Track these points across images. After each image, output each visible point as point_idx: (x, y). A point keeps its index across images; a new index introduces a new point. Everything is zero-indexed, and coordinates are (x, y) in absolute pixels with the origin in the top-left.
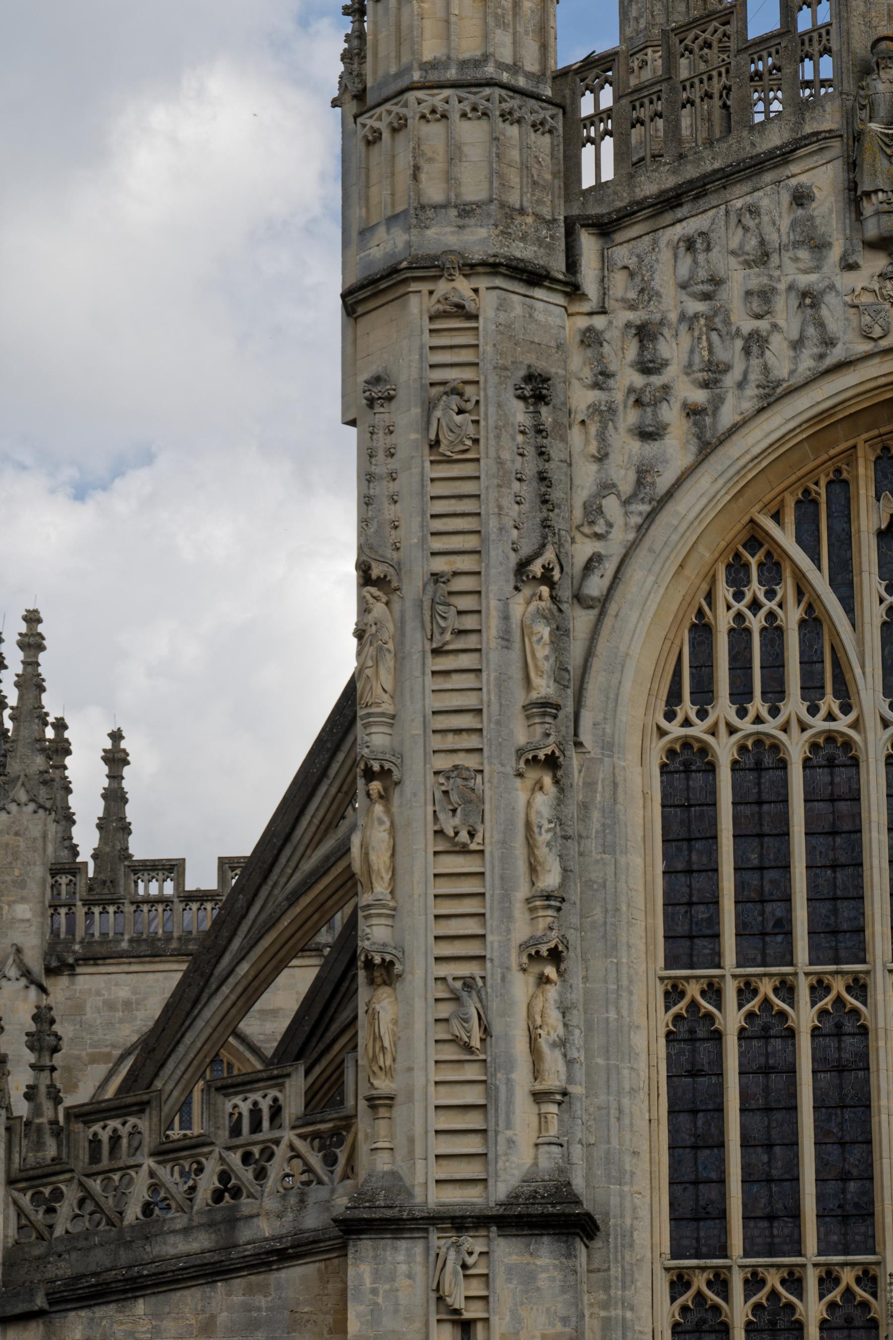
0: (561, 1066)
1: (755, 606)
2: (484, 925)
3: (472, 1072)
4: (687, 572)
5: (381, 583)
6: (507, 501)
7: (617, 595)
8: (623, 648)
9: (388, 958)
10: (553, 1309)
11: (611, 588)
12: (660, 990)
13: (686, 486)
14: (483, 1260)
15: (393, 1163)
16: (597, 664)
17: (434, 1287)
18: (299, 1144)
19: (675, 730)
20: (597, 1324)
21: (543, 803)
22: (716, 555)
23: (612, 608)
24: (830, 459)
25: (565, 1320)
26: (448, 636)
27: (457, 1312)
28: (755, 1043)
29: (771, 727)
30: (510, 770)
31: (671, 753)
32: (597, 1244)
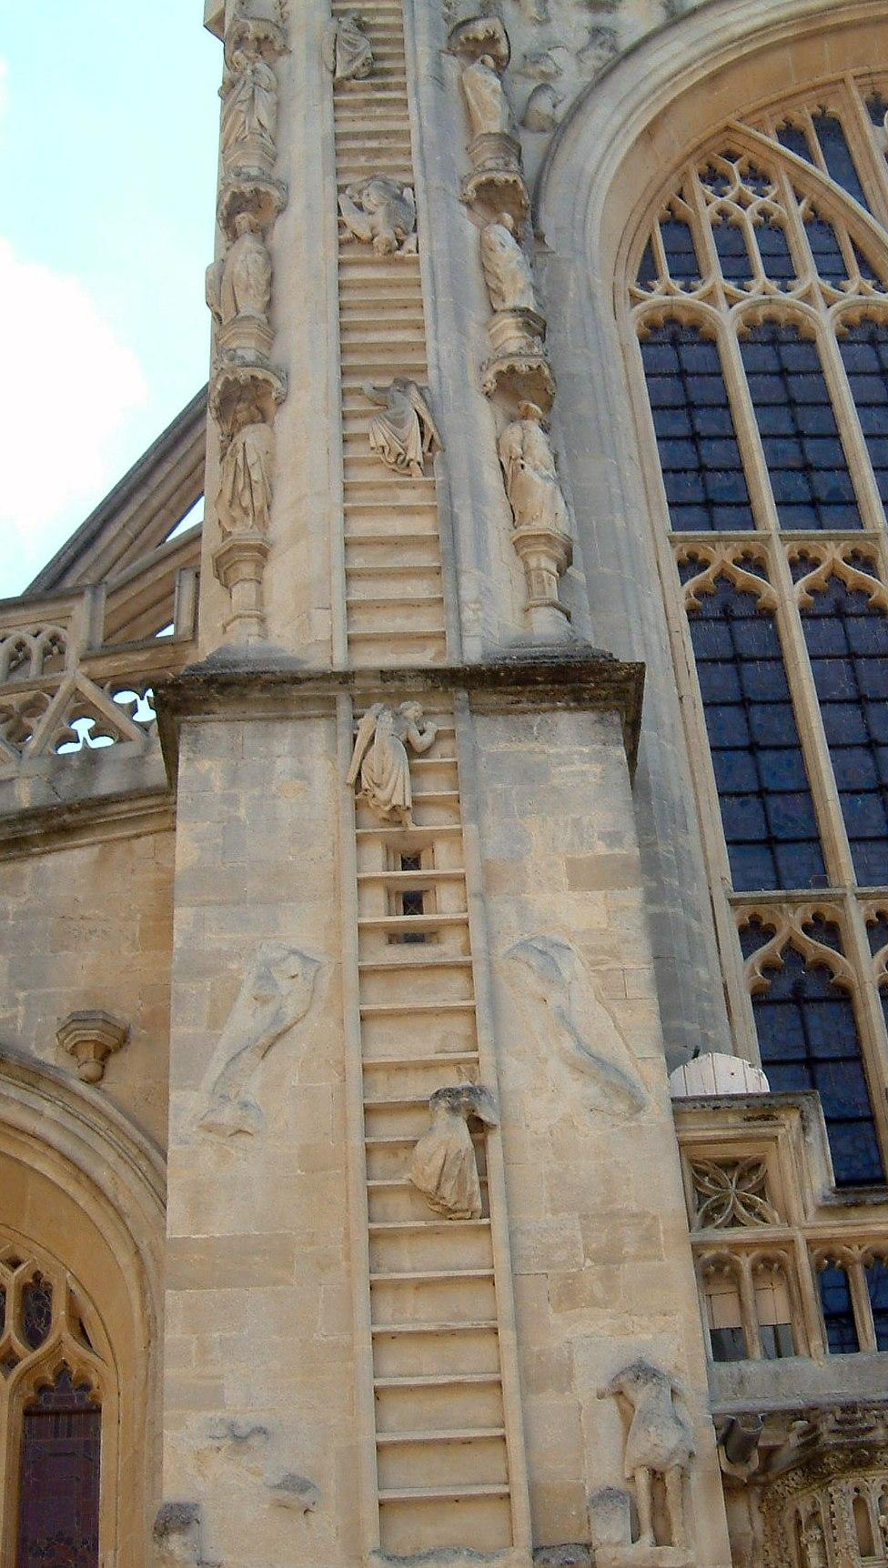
1: (742, 202)
2: (423, 335)
8: (590, 167)
9: (260, 374)
10: (585, 820)
13: (655, 44)
14: (445, 746)
15: (264, 635)
17: (352, 778)
19: (656, 298)
21: (501, 234)
22: (688, 148)
23: (571, 133)
24: (814, 88)
25: (613, 838)
26: (358, 63)
28: (824, 622)
31: (652, 326)
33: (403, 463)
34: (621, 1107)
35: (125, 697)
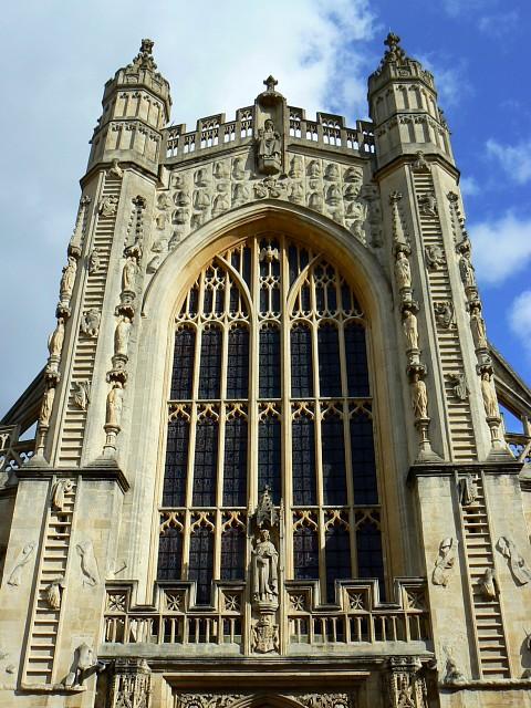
0: (119, 417)
3: (81, 417)
4: (192, 268)
5: (75, 255)
6: (124, 230)
7: (163, 268)
11: (160, 267)
12: (167, 406)
16: (152, 289)
18: (14, 453)
19: (182, 320)
20: (124, 525)
23: (160, 273)
25: (106, 515)
27: (60, 509)
29: (217, 320)
30: (113, 311)
32: (129, 493)
33: (80, 407)
34: (93, 583)
35: (23, 455)
